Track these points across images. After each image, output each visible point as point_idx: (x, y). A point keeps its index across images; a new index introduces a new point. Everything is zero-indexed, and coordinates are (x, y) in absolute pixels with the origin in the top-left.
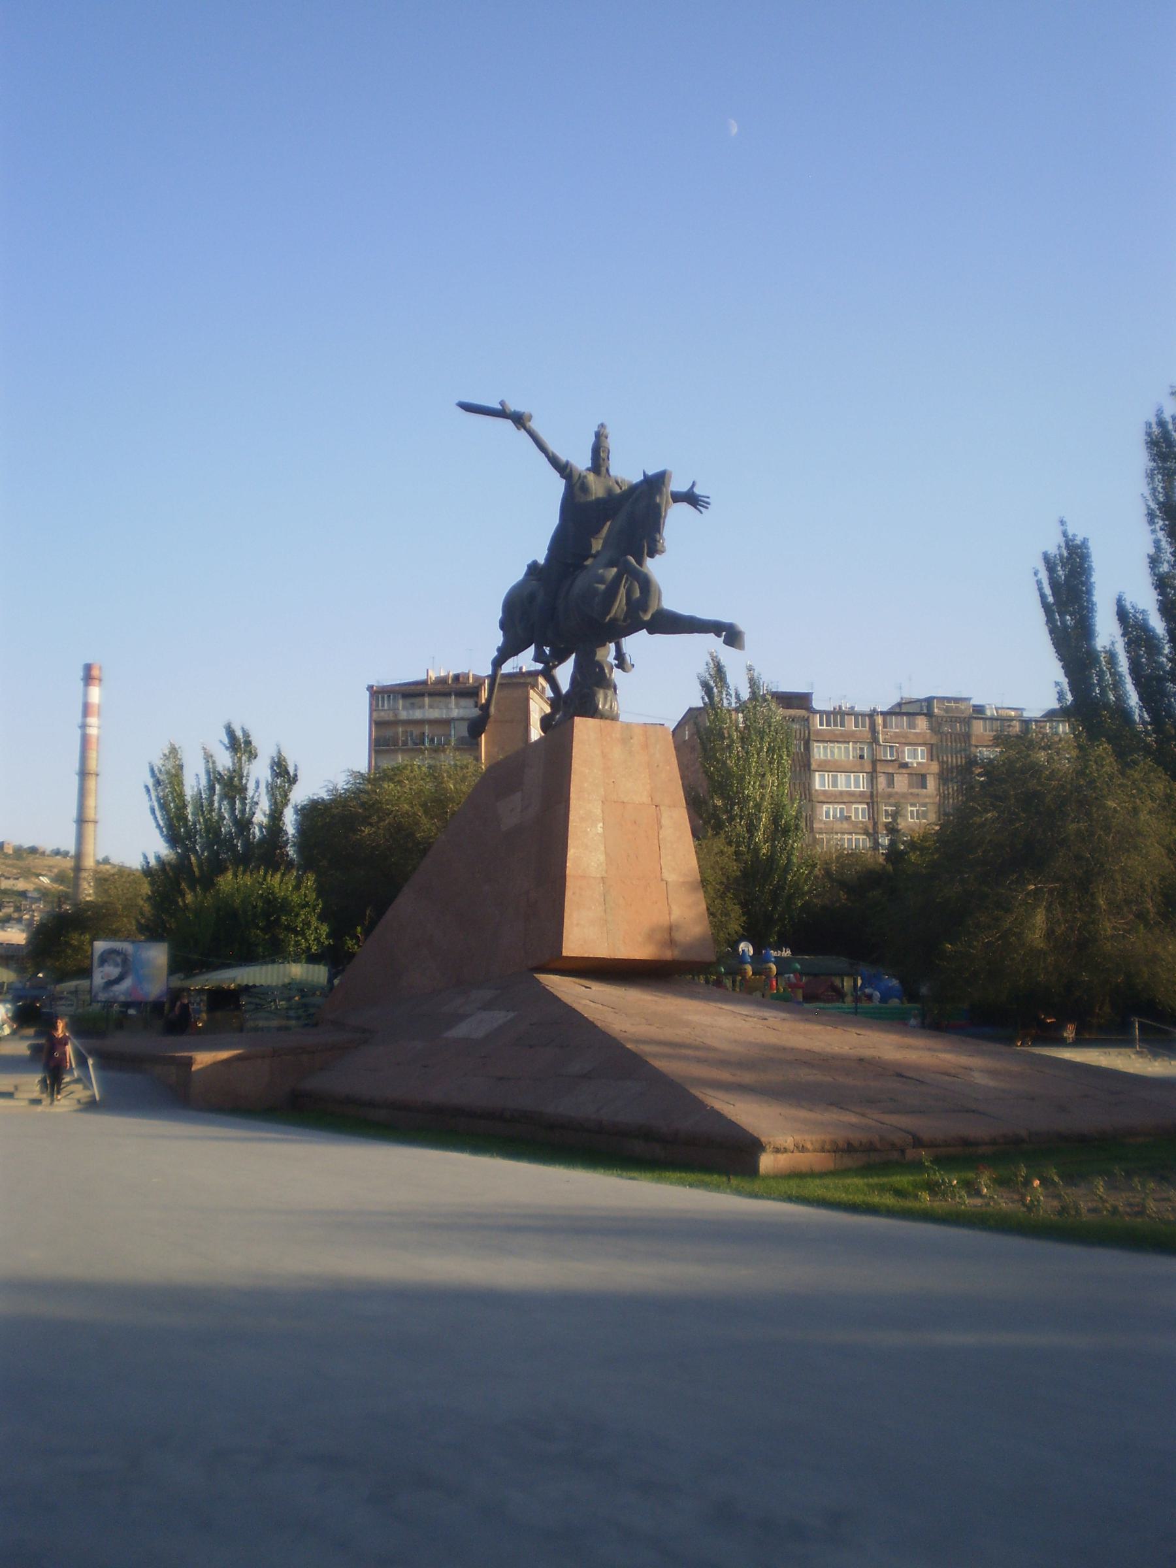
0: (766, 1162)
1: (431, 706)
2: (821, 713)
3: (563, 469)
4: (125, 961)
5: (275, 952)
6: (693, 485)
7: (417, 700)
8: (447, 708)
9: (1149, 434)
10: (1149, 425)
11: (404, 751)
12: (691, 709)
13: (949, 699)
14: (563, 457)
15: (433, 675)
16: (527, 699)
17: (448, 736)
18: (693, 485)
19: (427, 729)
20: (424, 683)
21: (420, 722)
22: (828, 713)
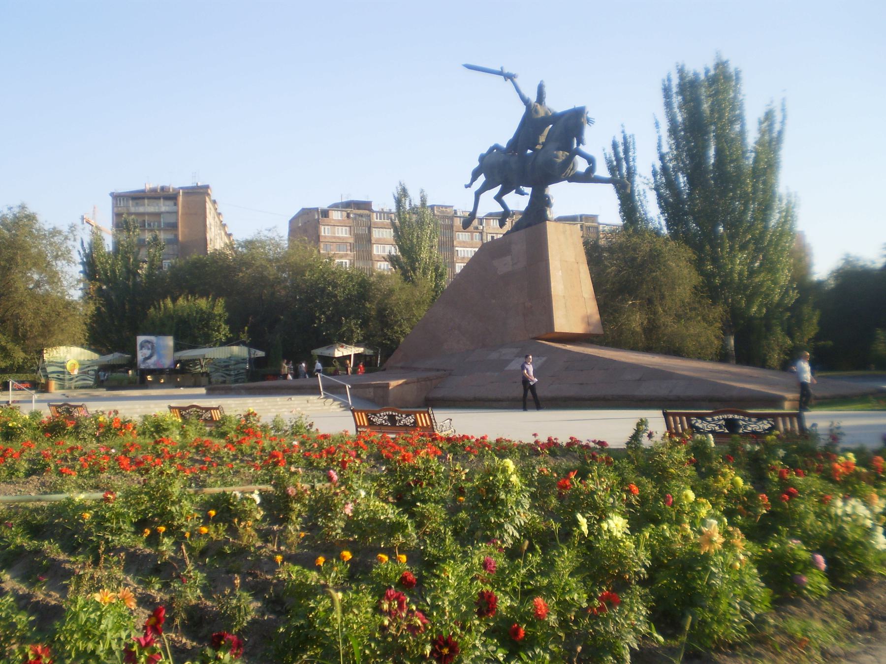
2: (377, 212)
3: (526, 102)
4: (153, 347)
5: (208, 341)
9: (664, 85)
10: (664, 81)
12: (303, 209)
13: (442, 206)
16: (205, 202)
17: (160, 222)
19: (146, 218)
20: (143, 191)
21: (143, 214)
22: (380, 213)
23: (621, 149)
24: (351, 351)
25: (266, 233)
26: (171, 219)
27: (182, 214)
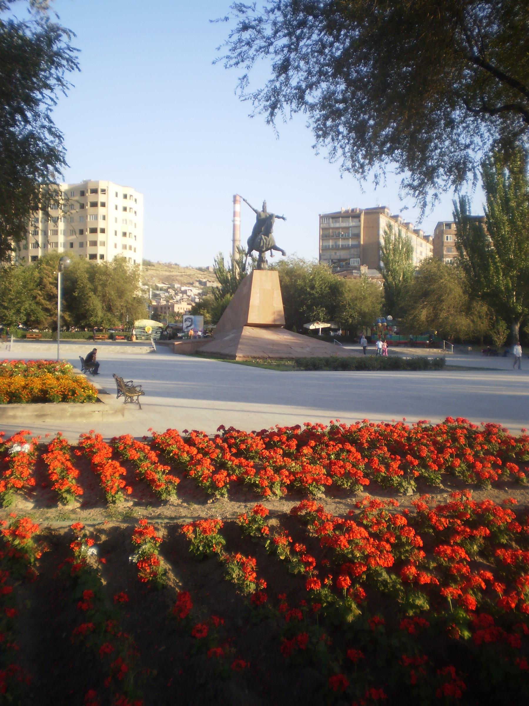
0: (237, 359)
1: (342, 222)
3: (256, 211)
4: (192, 321)
7: (337, 219)
8: (349, 222)
11: (332, 239)
14: (255, 208)
15: (344, 209)
17: (349, 233)
20: (340, 212)
21: (338, 228)
23: (458, 205)
24: (320, 326)
25: (292, 256)
26: (356, 231)
27: (364, 227)
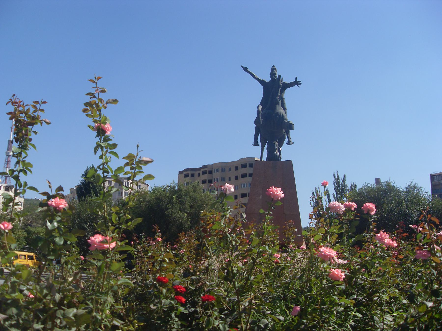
3: (262, 82)
6: (296, 78)
18: (296, 78)
